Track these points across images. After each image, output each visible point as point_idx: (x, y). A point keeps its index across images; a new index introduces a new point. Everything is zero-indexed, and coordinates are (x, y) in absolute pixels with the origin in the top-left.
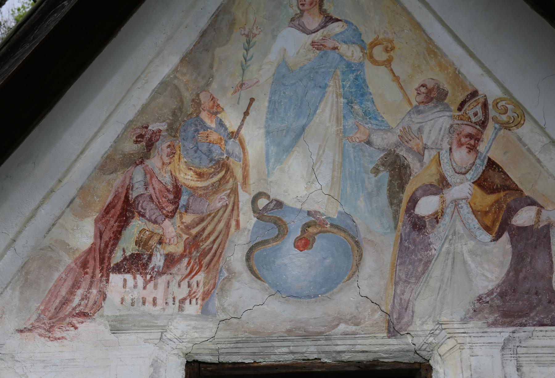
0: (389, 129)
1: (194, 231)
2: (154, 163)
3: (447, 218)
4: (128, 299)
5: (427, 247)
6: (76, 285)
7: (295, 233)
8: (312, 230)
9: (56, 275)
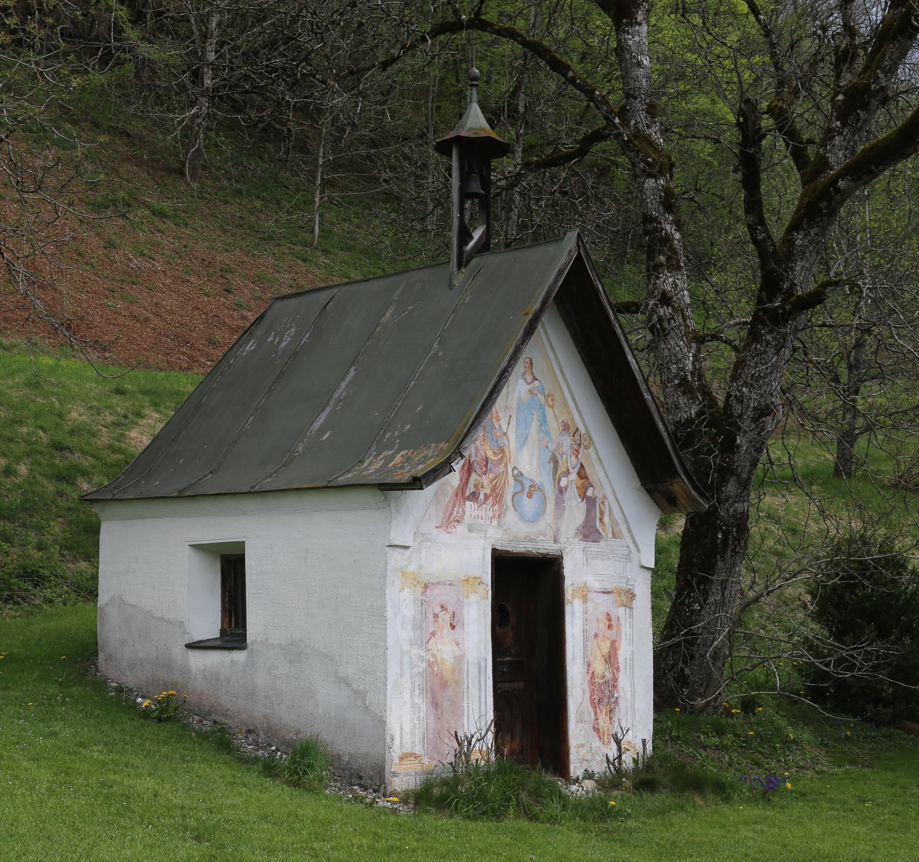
1: (494, 483)
4: (473, 514)
6: (454, 506)
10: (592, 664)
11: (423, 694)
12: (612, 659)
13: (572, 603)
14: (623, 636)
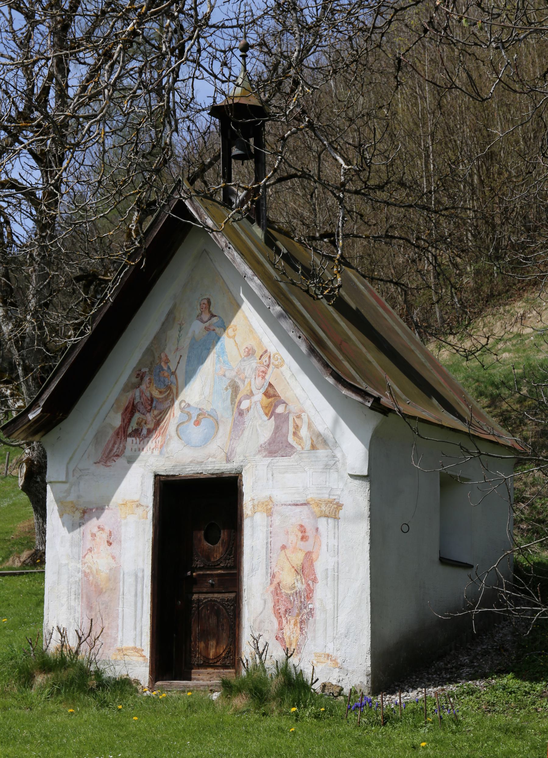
0: (233, 369)
1: (158, 418)
2: (143, 387)
3: (252, 410)
5: (244, 423)
6: (115, 443)
7: (194, 418)
8: (201, 417)
9: (108, 439)
10: (277, 575)
11: (78, 598)
12: (306, 571)
13: (252, 517)
14: (324, 547)
